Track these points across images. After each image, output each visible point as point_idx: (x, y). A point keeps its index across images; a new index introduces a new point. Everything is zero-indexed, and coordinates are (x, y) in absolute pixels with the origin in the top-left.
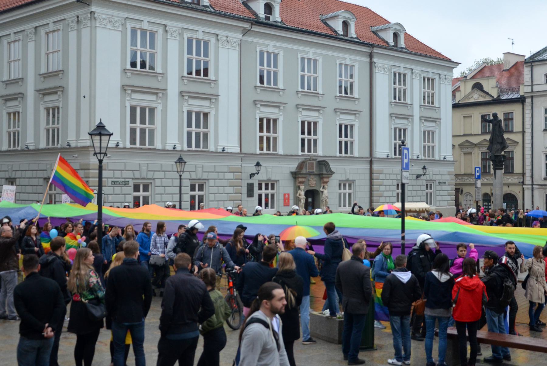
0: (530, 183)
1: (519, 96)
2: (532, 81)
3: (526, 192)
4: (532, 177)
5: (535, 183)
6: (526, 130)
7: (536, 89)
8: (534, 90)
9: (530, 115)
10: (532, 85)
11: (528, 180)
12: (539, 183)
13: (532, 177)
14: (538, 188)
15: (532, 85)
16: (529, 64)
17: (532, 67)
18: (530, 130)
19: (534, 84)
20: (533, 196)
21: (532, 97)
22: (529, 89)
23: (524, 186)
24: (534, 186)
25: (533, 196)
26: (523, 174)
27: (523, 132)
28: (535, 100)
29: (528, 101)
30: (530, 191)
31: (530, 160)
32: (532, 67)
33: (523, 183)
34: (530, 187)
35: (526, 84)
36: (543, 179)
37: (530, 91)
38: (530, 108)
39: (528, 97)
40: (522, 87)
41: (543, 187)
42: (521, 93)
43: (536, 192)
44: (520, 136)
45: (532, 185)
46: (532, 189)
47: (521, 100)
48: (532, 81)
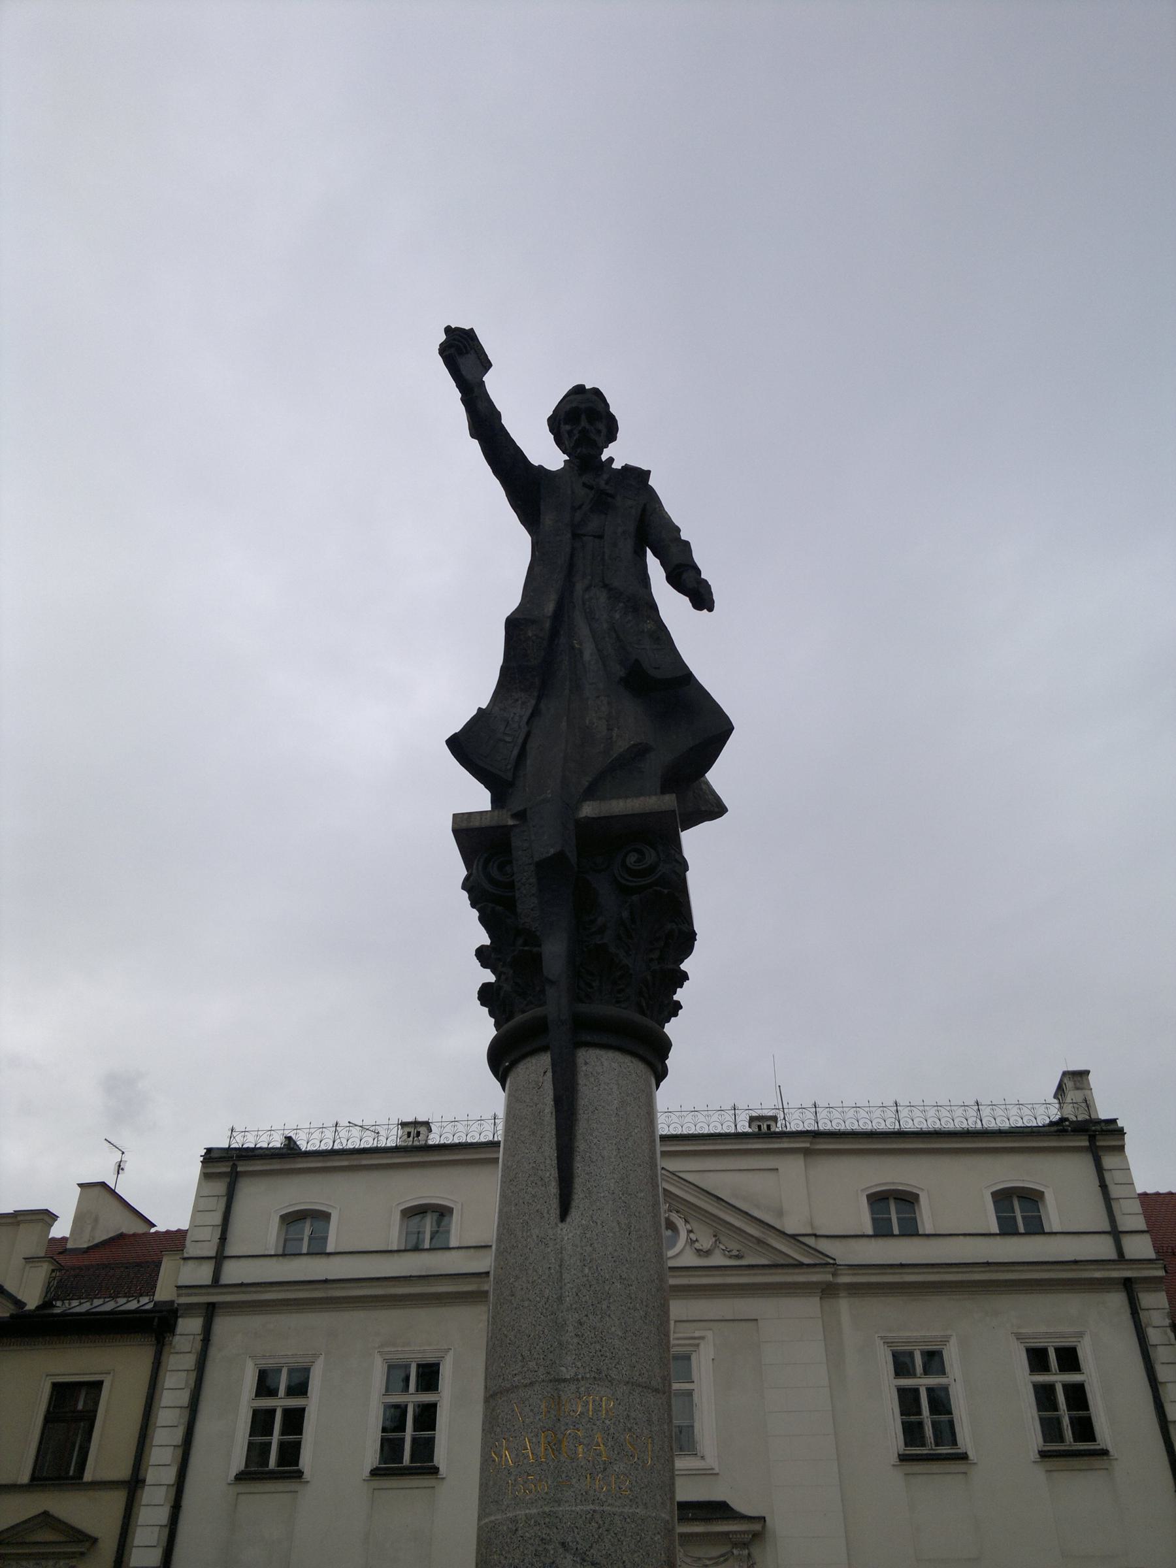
2: (223, 1239)
6: (151, 1476)
7: (233, 1272)
8: (226, 1279)
9: (184, 1398)
10: (220, 1258)
15: (220, 1258)
16: (225, 1168)
17: (233, 1180)
19: (231, 1250)
21: (210, 1312)
22: (202, 1274)
27: (134, 1484)
28: (223, 1325)
29: (189, 1326)
37: (208, 1280)
38: (189, 1361)
39: (190, 1309)
42: (164, 1292)
47: (157, 1326)
48: (223, 1239)
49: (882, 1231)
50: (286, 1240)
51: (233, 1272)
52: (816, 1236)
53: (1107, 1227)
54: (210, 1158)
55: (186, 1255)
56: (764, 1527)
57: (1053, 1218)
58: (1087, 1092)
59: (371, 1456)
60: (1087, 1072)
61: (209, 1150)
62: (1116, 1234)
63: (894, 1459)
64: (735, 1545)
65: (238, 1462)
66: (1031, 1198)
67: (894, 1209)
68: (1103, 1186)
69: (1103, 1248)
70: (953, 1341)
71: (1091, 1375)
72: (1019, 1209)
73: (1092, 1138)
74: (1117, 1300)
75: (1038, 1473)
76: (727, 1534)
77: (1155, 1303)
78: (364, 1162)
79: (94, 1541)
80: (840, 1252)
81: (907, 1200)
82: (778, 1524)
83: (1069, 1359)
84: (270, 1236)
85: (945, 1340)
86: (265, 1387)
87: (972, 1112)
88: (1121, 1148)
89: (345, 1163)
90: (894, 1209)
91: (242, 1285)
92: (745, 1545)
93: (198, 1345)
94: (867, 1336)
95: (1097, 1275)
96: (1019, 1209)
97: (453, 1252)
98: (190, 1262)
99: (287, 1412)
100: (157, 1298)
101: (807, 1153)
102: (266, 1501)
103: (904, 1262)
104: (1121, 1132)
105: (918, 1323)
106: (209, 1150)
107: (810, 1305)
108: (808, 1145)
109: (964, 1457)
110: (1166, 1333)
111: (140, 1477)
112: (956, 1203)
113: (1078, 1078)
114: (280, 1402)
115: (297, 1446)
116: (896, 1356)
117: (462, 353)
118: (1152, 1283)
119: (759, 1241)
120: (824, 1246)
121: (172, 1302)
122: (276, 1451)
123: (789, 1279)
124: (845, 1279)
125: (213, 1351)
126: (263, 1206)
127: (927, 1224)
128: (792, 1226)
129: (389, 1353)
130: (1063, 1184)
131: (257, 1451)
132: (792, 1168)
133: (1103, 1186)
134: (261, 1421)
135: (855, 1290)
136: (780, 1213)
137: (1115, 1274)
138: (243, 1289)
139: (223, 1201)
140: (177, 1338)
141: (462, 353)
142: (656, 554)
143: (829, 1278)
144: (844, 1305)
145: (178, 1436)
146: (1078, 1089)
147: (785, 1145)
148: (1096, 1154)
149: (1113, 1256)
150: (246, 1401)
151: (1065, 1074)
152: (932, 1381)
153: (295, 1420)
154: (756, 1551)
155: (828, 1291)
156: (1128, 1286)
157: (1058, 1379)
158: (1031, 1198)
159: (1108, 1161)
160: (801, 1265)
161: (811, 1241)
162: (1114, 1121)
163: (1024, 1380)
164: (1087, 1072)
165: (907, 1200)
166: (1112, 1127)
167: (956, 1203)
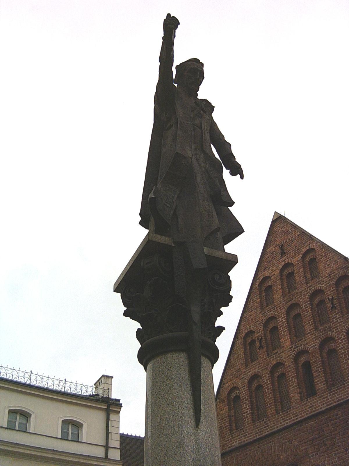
53: (103, 443)
57: (84, 437)
60: (112, 377)
62: (107, 447)
69: (100, 452)
73: (108, 406)
81: (26, 415)
87: (62, 384)
104: (120, 406)
113: (106, 379)
117: (171, 24)
130: (92, 422)
141: (171, 24)
142: (212, 144)
148: (108, 412)
151: (103, 376)
158: (78, 426)
159: (112, 417)
162: (119, 400)
164: (112, 377)
166: (118, 403)
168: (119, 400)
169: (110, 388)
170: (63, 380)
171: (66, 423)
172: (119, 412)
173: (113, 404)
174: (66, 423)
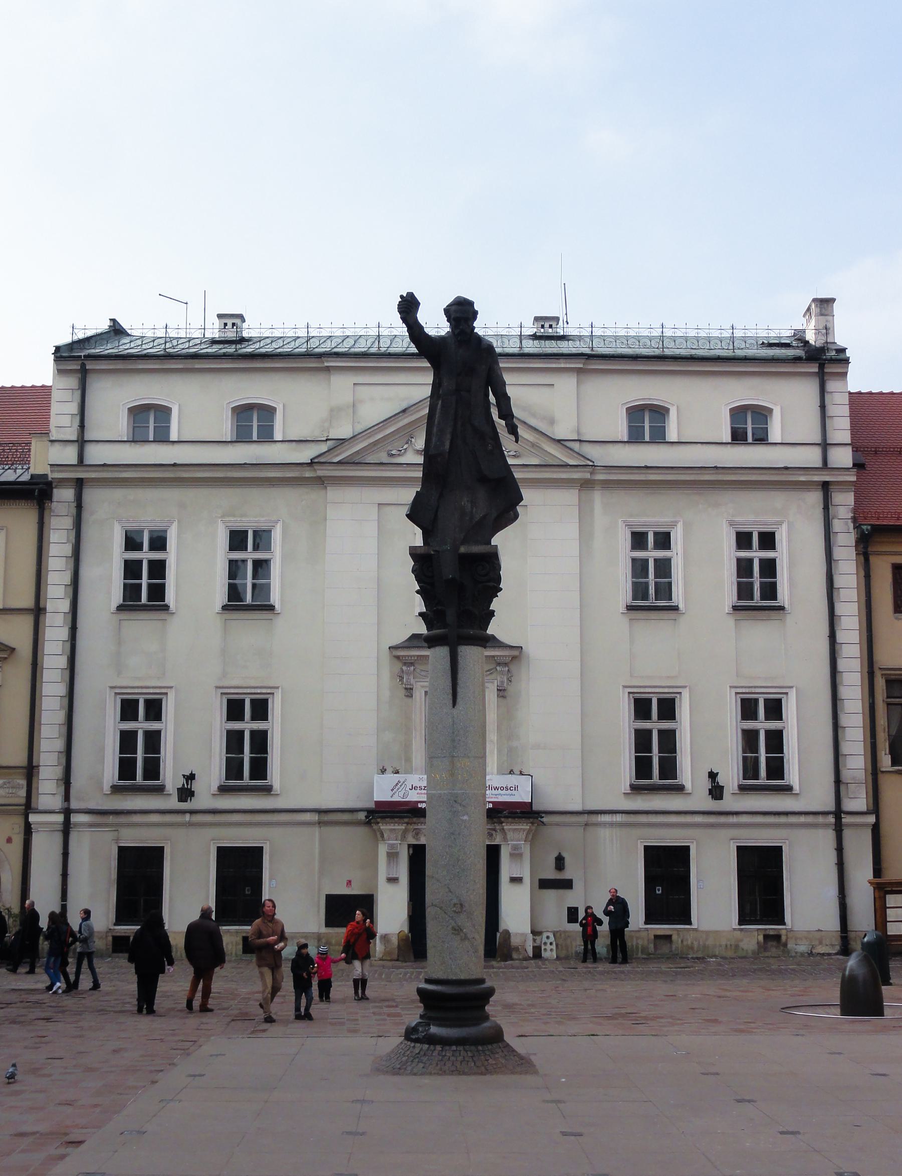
0: (57, 802)
1: (26, 478)
2: (82, 426)
3: (37, 840)
4: (66, 780)
5: (74, 805)
6: (50, 607)
7: (96, 454)
8: (88, 461)
9: (68, 550)
10: (82, 442)
11: (48, 792)
12: (92, 805)
13: (66, 780)
14: (91, 825)
15: (82, 442)
16: (76, 366)
17: (84, 375)
18: (65, 606)
20: (65, 854)
21: (80, 484)
22: (69, 455)
23: (32, 818)
24: (75, 818)
25: (65, 854)
26: (30, 771)
27: (38, 611)
28: (91, 495)
29: (64, 496)
30: (58, 838)
31: (60, 717)
32: (84, 375)
33: (28, 807)
34: (60, 818)
35: (54, 435)
36: (107, 789)
37: (74, 461)
39: (62, 482)
40: (37, 446)
41: (111, 819)
43: (81, 844)
44: (25, 624)
45: (67, 812)
46: (66, 829)
48: (82, 426)
49: (635, 437)
50: (134, 427)
51: (96, 454)
52: (580, 441)
53: (818, 439)
54: (62, 357)
55: (52, 438)
56: (521, 652)
58: (830, 318)
59: (220, 596)
61: (58, 349)
62: (825, 445)
63: (622, 608)
64: (499, 664)
65: (117, 596)
66: (762, 414)
67: (647, 421)
68: (823, 407)
69: (813, 457)
70: (680, 526)
71: (782, 554)
72: (748, 425)
73: (822, 367)
74: (815, 498)
75: (730, 622)
76: (493, 657)
77: (844, 502)
78: (197, 366)
79: (13, 650)
80: (597, 454)
82: (532, 649)
83: (768, 540)
84: (121, 426)
85: (674, 524)
86: (132, 543)
88: (845, 374)
89: (180, 366)
90: (647, 421)
91: (105, 465)
92: (506, 664)
93: (74, 511)
94: (614, 523)
95: (802, 478)
96: (748, 425)
97: (278, 444)
98: (56, 444)
99: (151, 563)
100: (32, 471)
101: (579, 371)
102: (141, 627)
103: (649, 465)
104: (846, 361)
105: (652, 513)
106: (58, 349)
107: (571, 496)
108: (581, 366)
109: (675, 608)
110: (847, 524)
111: (41, 606)
112: (700, 413)
113: (824, 305)
114: (145, 555)
115: (162, 587)
116: (634, 534)
118: (843, 485)
119: (533, 445)
120: (588, 450)
121: (46, 476)
122: (145, 589)
123: (555, 476)
124: (600, 477)
125: (85, 515)
126: (114, 400)
127: (672, 435)
128: (563, 431)
129: (230, 521)
131: (131, 592)
132: (565, 386)
133: (823, 407)
134: (132, 569)
135: (607, 485)
136: (552, 422)
137: (816, 478)
138: (106, 468)
139: (78, 394)
140: (54, 505)
143: (588, 476)
144: (598, 497)
145: (67, 578)
146: (822, 315)
147: (563, 366)
149: (819, 464)
150: (118, 555)
152: (661, 554)
153: (158, 569)
154: (513, 667)
155: (586, 485)
156: (825, 486)
157: (756, 554)
158: (762, 414)
160: (567, 465)
161: (576, 446)
162: (843, 350)
163: (729, 554)
164: (833, 300)
165: (659, 412)
166: (841, 356)
167: (700, 413)
168: (843, 350)
169: (829, 325)
170: (729, 326)
171: (738, 413)
172: (846, 373)
173: (832, 361)
174: (738, 413)
